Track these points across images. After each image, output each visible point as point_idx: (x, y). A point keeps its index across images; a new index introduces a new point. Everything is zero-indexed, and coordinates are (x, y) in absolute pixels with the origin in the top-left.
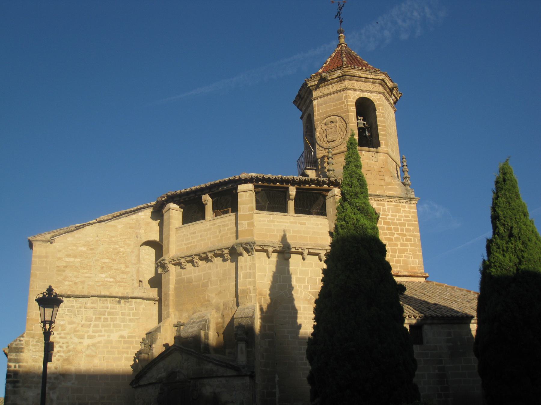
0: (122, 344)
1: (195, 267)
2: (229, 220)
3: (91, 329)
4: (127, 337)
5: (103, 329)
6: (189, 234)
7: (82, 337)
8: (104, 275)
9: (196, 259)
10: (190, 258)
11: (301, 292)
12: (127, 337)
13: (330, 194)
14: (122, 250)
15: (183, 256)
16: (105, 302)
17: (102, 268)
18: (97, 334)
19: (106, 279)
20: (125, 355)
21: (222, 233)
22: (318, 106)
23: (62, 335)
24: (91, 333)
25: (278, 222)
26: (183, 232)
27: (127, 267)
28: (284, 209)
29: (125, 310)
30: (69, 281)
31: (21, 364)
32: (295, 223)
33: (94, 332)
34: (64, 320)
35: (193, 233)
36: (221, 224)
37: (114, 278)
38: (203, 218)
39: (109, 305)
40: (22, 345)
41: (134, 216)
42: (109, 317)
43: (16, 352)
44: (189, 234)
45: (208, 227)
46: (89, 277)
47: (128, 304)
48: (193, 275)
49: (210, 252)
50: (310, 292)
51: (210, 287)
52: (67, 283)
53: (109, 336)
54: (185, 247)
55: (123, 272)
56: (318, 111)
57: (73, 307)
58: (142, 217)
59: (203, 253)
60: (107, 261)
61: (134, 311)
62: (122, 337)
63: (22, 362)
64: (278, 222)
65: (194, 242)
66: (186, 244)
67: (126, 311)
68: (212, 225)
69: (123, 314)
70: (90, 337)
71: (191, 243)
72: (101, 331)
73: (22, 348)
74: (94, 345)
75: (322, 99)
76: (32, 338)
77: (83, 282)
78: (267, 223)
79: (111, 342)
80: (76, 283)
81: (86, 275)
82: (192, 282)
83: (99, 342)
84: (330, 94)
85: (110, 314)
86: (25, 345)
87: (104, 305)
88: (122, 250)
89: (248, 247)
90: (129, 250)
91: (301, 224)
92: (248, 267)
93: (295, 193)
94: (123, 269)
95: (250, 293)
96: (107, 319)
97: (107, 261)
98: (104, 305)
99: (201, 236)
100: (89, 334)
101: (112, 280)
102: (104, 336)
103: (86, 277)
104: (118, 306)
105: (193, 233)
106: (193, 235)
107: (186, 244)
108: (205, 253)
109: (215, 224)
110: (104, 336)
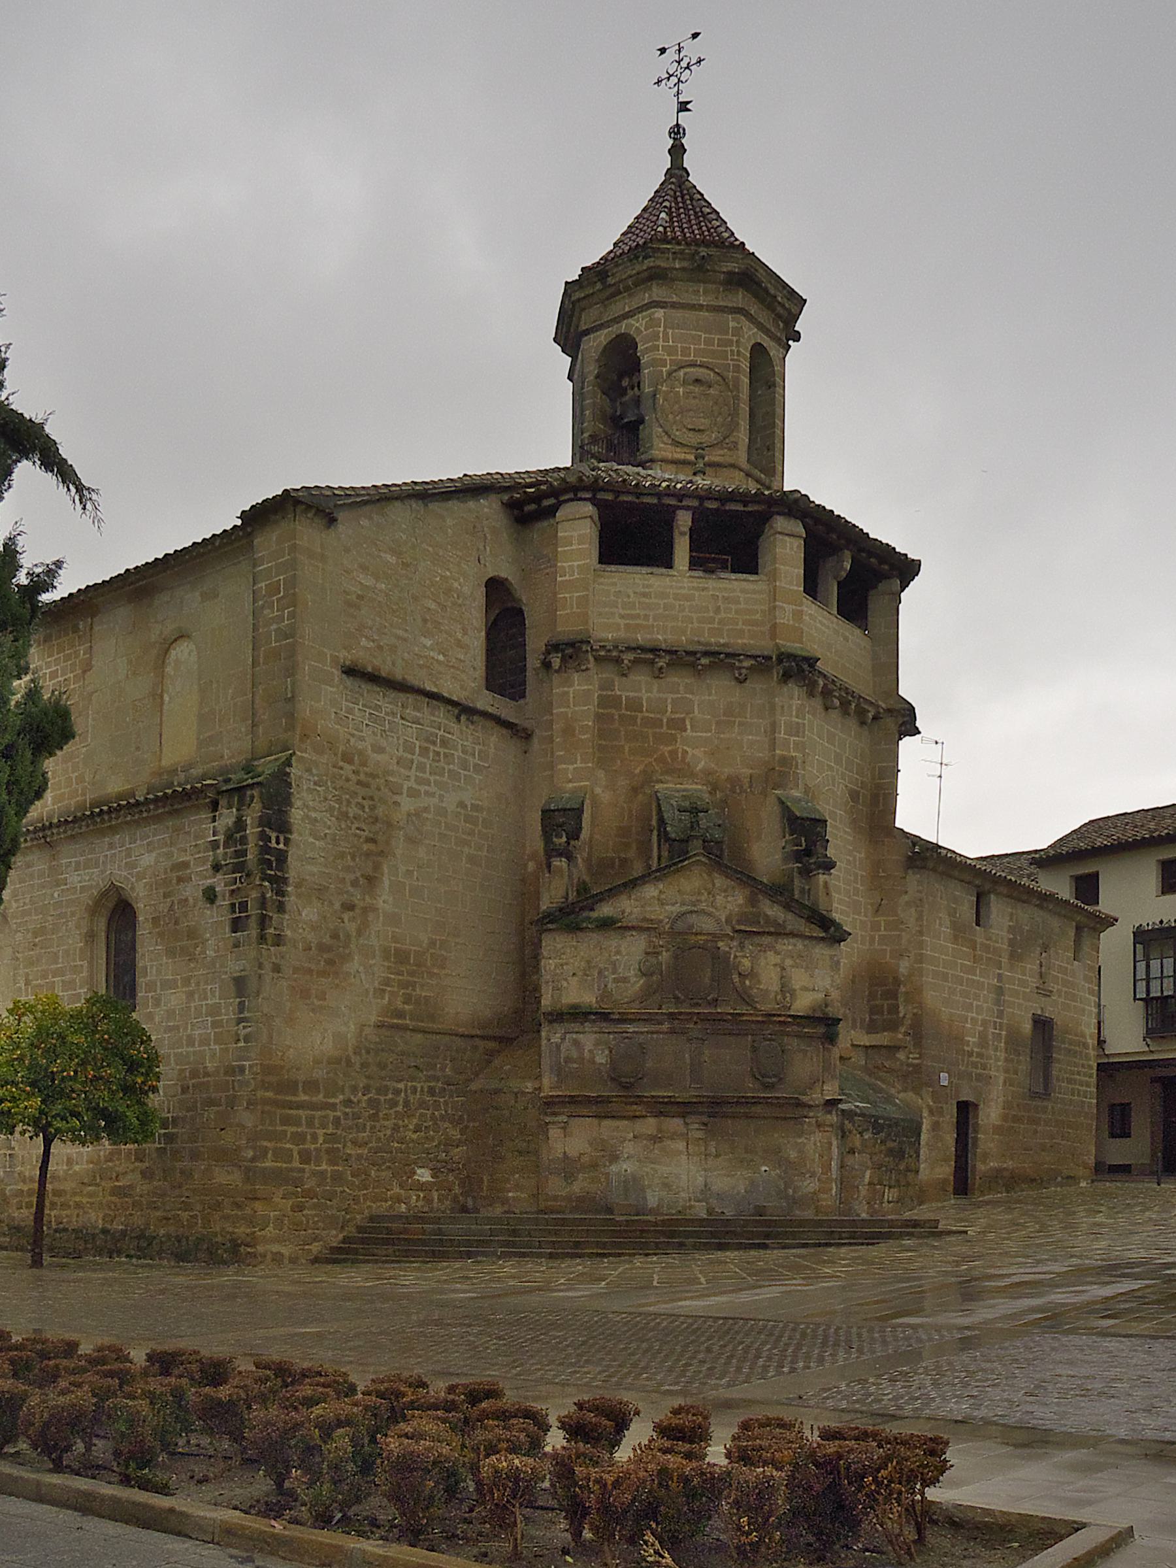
5: (432, 778)
8: (429, 643)
14: (456, 585)
18: (423, 788)
19: (432, 654)
21: (723, 615)
22: (665, 327)
23: (362, 777)
25: (820, 622)
26: (615, 584)
27: (465, 633)
28: (667, 562)
34: (362, 739)
35: (644, 595)
37: (444, 656)
38: (669, 565)
42: (442, 751)
46: (405, 640)
48: (645, 696)
49: (706, 654)
53: (441, 797)
54: (622, 622)
60: (433, 606)
64: (820, 622)
65: (646, 617)
66: (622, 617)
71: (638, 616)
74: (417, 815)
75: (678, 314)
77: (393, 649)
79: (442, 812)
80: (380, 648)
81: (400, 633)
82: (642, 711)
83: (426, 809)
84: (701, 307)
85: (444, 743)
89: (805, 667)
90: (466, 590)
94: (459, 636)
95: (797, 767)
96: (438, 754)
97: (433, 606)
99: (666, 607)
101: (441, 657)
102: (433, 795)
103: (398, 638)
104: (454, 726)
105: (644, 595)
107: (622, 617)
108: (693, 653)
109: (704, 589)
110: (433, 795)
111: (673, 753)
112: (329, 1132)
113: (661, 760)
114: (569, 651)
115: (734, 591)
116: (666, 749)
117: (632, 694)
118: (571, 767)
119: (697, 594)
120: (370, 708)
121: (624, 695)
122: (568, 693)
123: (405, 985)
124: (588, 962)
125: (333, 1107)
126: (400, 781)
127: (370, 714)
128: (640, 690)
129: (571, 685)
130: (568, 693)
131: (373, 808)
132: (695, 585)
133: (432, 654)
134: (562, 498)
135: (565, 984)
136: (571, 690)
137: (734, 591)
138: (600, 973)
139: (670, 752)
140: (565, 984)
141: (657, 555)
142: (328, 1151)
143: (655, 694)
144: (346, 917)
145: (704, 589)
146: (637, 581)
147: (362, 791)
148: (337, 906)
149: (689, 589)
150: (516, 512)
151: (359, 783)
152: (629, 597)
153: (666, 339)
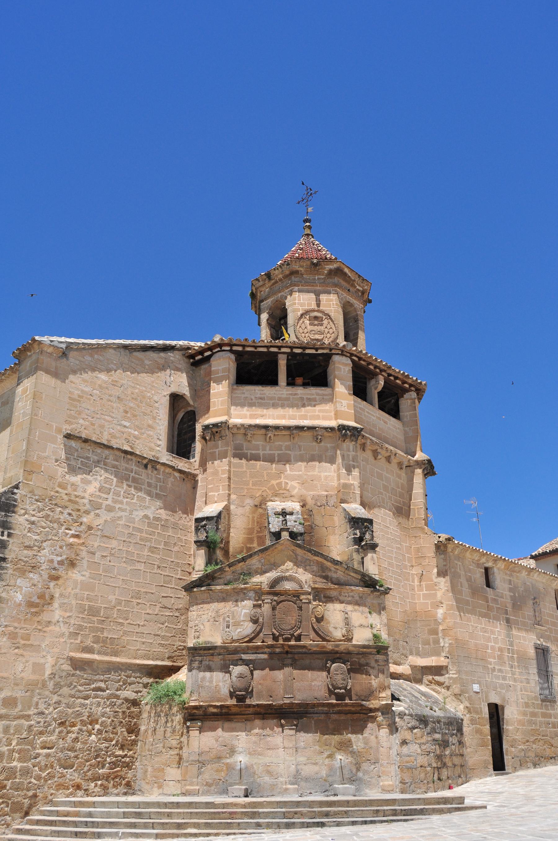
0: (146, 528)
2: (318, 394)
3: (110, 496)
4: (152, 518)
5: (125, 500)
6: (253, 398)
7: (98, 506)
11: (387, 503)
12: (152, 518)
13: (406, 396)
16: (130, 463)
17: (126, 412)
18: (117, 506)
20: (148, 544)
23: (73, 498)
24: (109, 502)
26: (244, 393)
29: (152, 479)
30: (83, 419)
31: (12, 531)
32: (379, 419)
33: (115, 501)
35: (261, 398)
36: (305, 397)
39: (135, 468)
40: (15, 500)
41: (162, 354)
43: (6, 511)
44: (253, 398)
45: (285, 396)
47: (155, 472)
50: (393, 504)
51: (289, 472)
52: (81, 421)
53: (131, 512)
55: (149, 426)
56: (299, 300)
57: (88, 458)
58: (171, 358)
61: (162, 484)
62: (146, 516)
63: (14, 530)
67: (153, 481)
68: (291, 394)
69: (149, 485)
70: (110, 509)
72: (121, 502)
73: (15, 506)
76: (30, 492)
78: (359, 409)
80: (93, 424)
83: (120, 518)
86: (19, 500)
87: (128, 466)
88: (149, 395)
91: (385, 422)
92: (351, 457)
93: (383, 383)
95: (354, 490)
98: (128, 466)
100: (107, 503)
105: (261, 398)
106: (260, 401)
109: (296, 394)
111: (279, 484)
112: (22, 737)
113: (272, 488)
114: (215, 430)
115: (313, 395)
116: (274, 482)
117: (253, 452)
118: (216, 494)
119: (291, 397)
120: (81, 457)
122: (215, 452)
123: (93, 629)
124: (217, 612)
125: (28, 717)
126: (101, 501)
127: (81, 461)
129: (217, 448)
130: (215, 452)
131: (80, 516)
132: (290, 392)
133: (130, 430)
134: (214, 351)
135: (202, 627)
136: (217, 450)
137: (313, 395)
138: (224, 619)
139: (277, 484)
140: (202, 627)
141: (270, 380)
142: (20, 751)
144: (52, 584)
145: (296, 394)
146: (257, 391)
147: (71, 506)
148: (46, 576)
149: (287, 394)
150: (191, 360)
151: (70, 500)
152: (252, 400)
153: (299, 300)
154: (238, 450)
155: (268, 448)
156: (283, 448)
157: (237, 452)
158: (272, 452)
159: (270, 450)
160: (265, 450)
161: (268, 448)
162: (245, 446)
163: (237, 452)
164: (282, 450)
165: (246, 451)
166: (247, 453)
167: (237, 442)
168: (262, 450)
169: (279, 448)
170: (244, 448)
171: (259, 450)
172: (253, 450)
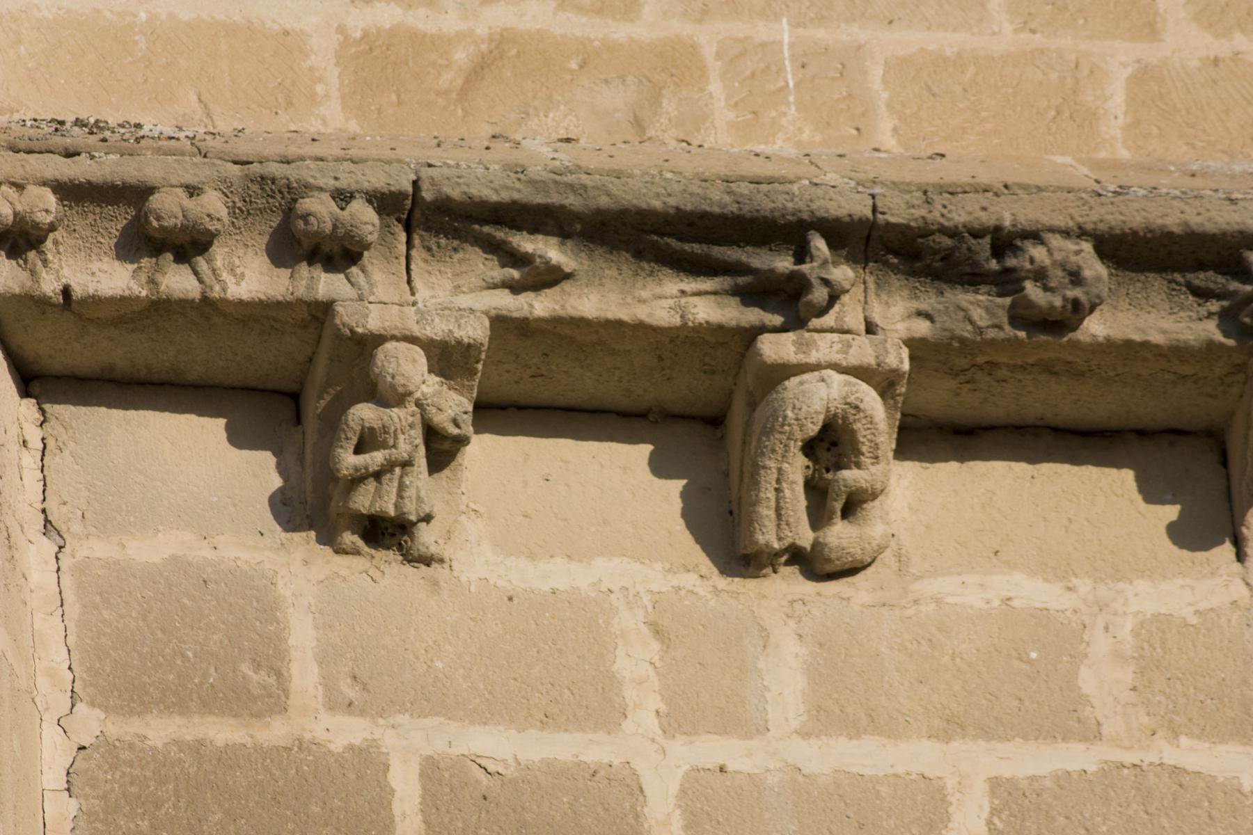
1: (737, 555)
9: (847, 352)
10: (672, 301)
15: (472, 166)
59: (1139, 253)
117: (500, 746)
121: (406, 749)
128: (605, 711)
143: (785, 746)
154: (178, 701)
155: (785, 678)
156: (1102, 680)
157: (160, 730)
158: (872, 757)
159: (826, 717)
160: (738, 719)
161: (785, 678)
162: (302, 636)
163: (160, 730)
164: (1092, 734)
165: (342, 733)
166: (368, 763)
167: (149, 550)
168: (679, 720)
169: (1026, 686)
170: (305, 676)
171: (605, 711)
172: (488, 712)
